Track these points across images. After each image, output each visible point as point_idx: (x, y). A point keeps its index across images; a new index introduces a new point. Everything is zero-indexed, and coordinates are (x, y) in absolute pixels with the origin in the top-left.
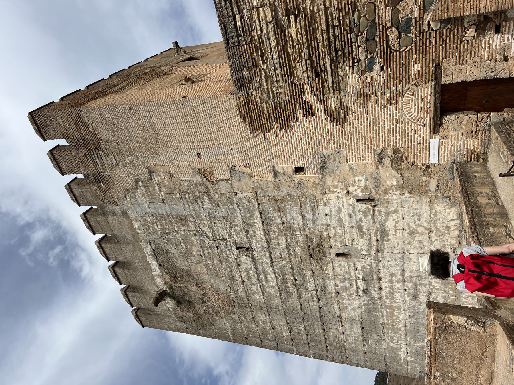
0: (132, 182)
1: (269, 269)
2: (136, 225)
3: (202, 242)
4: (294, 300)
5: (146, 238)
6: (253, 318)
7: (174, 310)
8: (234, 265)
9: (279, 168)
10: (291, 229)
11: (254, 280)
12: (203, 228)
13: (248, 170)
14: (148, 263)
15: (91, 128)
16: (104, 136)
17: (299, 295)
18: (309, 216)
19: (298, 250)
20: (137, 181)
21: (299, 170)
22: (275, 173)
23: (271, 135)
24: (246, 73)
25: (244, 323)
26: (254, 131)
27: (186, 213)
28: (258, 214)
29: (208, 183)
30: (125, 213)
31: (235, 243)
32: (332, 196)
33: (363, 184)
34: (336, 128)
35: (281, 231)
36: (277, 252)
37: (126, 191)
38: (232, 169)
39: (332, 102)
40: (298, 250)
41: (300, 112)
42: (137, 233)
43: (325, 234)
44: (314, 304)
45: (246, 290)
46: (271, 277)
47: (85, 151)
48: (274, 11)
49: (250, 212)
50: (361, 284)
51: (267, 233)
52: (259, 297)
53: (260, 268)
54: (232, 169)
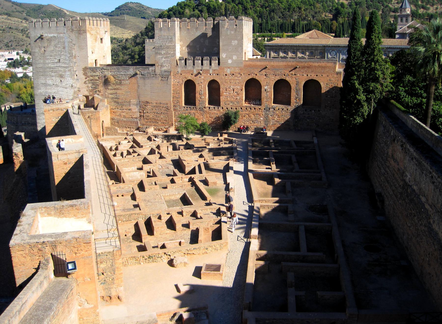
0: (72, 39)
1: (55, 65)
2: (62, 35)
3: (59, 51)
4: (48, 70)
5: (59, 36)
9: (77, 72)
11: (51, 61)
16: (82, 36)
17: (50, 71)
18: (68, 76)
19: (61, 73)
22: (76, 71)
23: (82, 71)
30: (64, 33)
36: (59, 68)
37: (70, 36)
39: (87, 82)
40: (61, 73)
44: (48, 74)
45: (48, 59)
46: (53, 66)
49: (68, 65)
50: (55, 84)
51: (64, 67)
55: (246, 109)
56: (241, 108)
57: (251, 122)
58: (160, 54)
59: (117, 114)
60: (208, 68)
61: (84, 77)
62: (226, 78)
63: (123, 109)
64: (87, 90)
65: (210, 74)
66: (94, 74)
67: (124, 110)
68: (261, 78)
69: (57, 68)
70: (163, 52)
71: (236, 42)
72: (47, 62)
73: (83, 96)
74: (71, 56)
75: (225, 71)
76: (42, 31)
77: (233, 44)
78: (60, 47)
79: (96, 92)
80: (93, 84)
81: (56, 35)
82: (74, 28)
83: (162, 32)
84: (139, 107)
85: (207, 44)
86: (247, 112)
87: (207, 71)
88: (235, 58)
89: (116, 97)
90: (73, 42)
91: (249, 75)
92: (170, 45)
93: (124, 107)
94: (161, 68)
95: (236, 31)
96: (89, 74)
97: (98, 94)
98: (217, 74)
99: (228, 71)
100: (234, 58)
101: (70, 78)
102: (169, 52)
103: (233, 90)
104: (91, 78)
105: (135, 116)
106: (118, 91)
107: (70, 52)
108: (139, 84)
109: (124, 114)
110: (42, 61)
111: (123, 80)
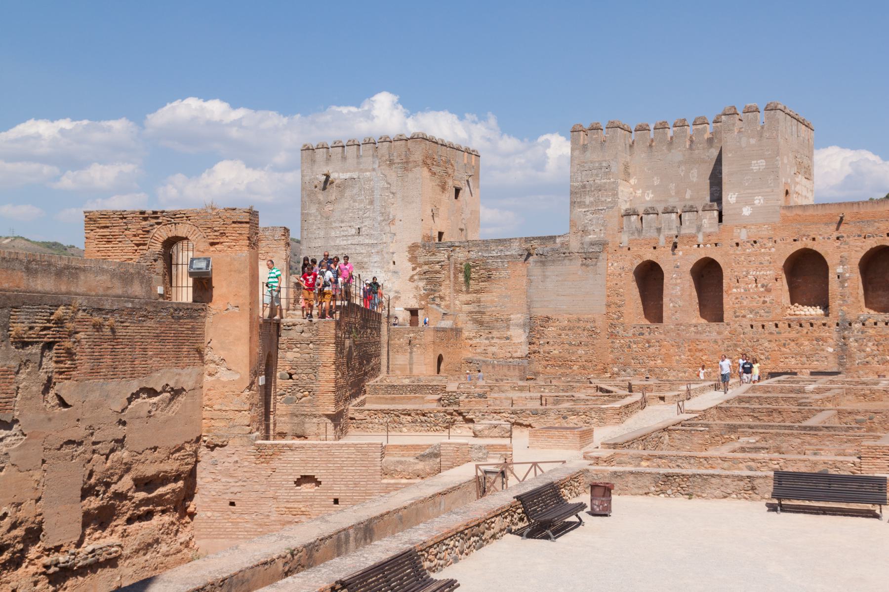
0: (389, 181)
1: (349, 242)
2: (367, 173)
5: (361, 177)
6: (320, 228)
7: (317, 179)
8: (350, 224)
10: (370, 256)
11: (343, 233)
12: (368, 213)
13: (394, 242)
14: (346, 172)
15: (413, 169)
16: (410, 175)
18: (376, 265)
19: (360, 258)
20: (390, 185)
21: (394, 263)
22: (393, 253)
23: (407, 254)
24: (427, 248)
25: (315, 222)
26: (409, 247)
27: (375, 205)
28: (376, 242)
29: (390, 221)
30: (374, 170)
31: (361, 228)
32: (384, 275)
33: (388, 286)
34: (408, 278)
35: (368, 252)
36: (358, 248)
37: (386, 176)
38: (395, 234)
39: (416, 277)
40: (360, 258)
41: (414, 266)
42: (363, 172)
43: (368, 270)
45: (336, 227)
46: (345, 243)
47: (404, 161)
48: (443, 261)
49: (377, 239)
51: (367, 245)
52: (333, 234)
53: (350, 238)
54: (395, 234)
55: (789, 326)
56: (776, 326)
57: (804, 359)
58: (581, 204)
59: (479, 351)
60: (693, 231)
61: (410, 266)
62: (738, 252)
63: (493, 338)
64: (415, 297)
65: (699, 246)
66: (433, 259)
67: (495, 341)
68: (826, 248)
69: (353, 247)
70: (588, 200)
71: (762, 163)
72: (333, 234)
73: (405, 309)
74: (384, 220)
75: (735, 234)
76: (328, 168)
77: (755, 168)
78: (361, 201)
79: (433, 299)
80: (430, 281)
81: (355, 175)
82: (395, 158)
83: (588, 154)
84: (527, 331)
85: (695, 180)
86: (793, 334)
87: (692, 238)
88: (758, 201)
89: (477, 309)
90: (394, 189)
91: (795, 240)
92: (605, 183)
93: (495, 333)
94: (582, 236)
95: (761, 137)
96: (421, 260)
97: (438, 305)
98: (716, 245)
99: (743, 235)
100: (756, 202)
101: (379, 270)
102: (603, 199)
103: (756, 280)
104: (426, 268)
105: (518, 354)
106: (484, 297)
107: (383, 211)
108: (532, 278)
109: (494, 349)
110: (322, 233)
111: (496, 269)
